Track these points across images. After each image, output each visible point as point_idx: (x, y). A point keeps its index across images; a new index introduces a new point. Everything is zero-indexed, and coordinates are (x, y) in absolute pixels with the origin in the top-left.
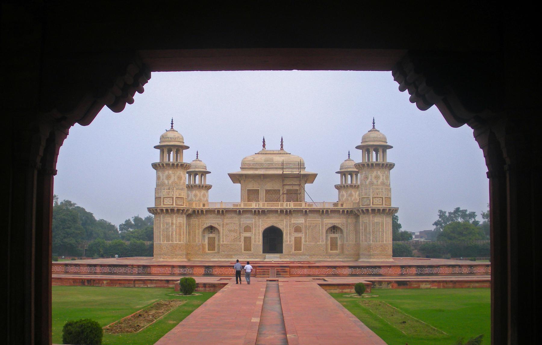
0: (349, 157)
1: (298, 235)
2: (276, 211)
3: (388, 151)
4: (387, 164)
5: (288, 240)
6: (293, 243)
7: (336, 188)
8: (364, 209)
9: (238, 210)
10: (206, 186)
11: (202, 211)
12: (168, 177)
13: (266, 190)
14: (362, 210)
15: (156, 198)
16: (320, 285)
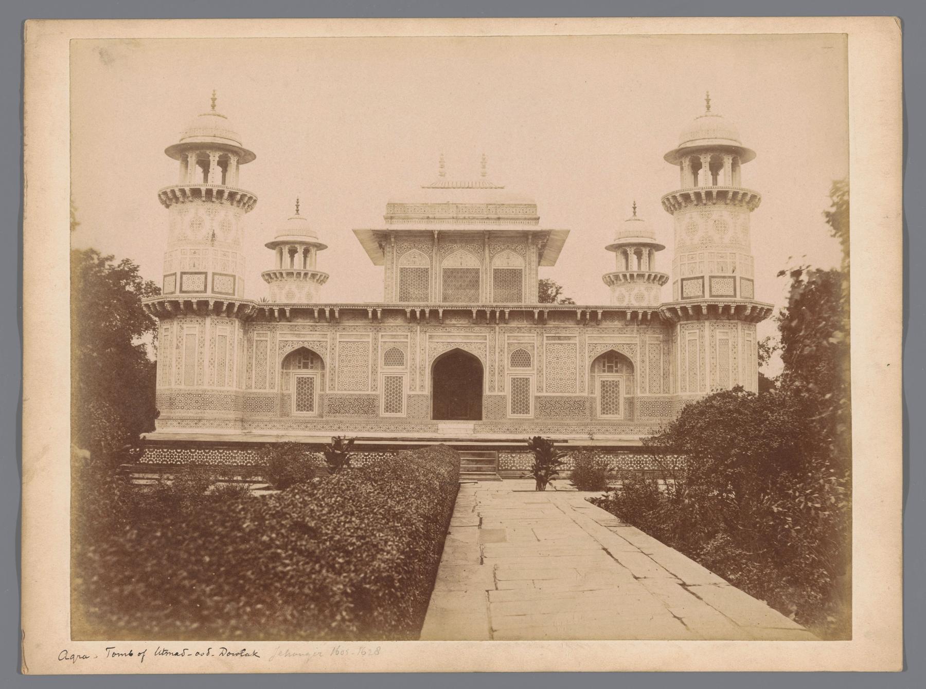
0: (635, 213)
1: (521, 372)
2: (465, 313)
3: (745, 168)
4: (745, 194)
5: (496, 386)
6: (508, 392)
7: (606, 283)
8: (689, 306)
9: (370, 310)
10: (314, 276)
11: (282, 312)
12: (196, 224)
13: (446, 271)
14: (684, 309)
15: (165, 276)
16: (593, 501)
